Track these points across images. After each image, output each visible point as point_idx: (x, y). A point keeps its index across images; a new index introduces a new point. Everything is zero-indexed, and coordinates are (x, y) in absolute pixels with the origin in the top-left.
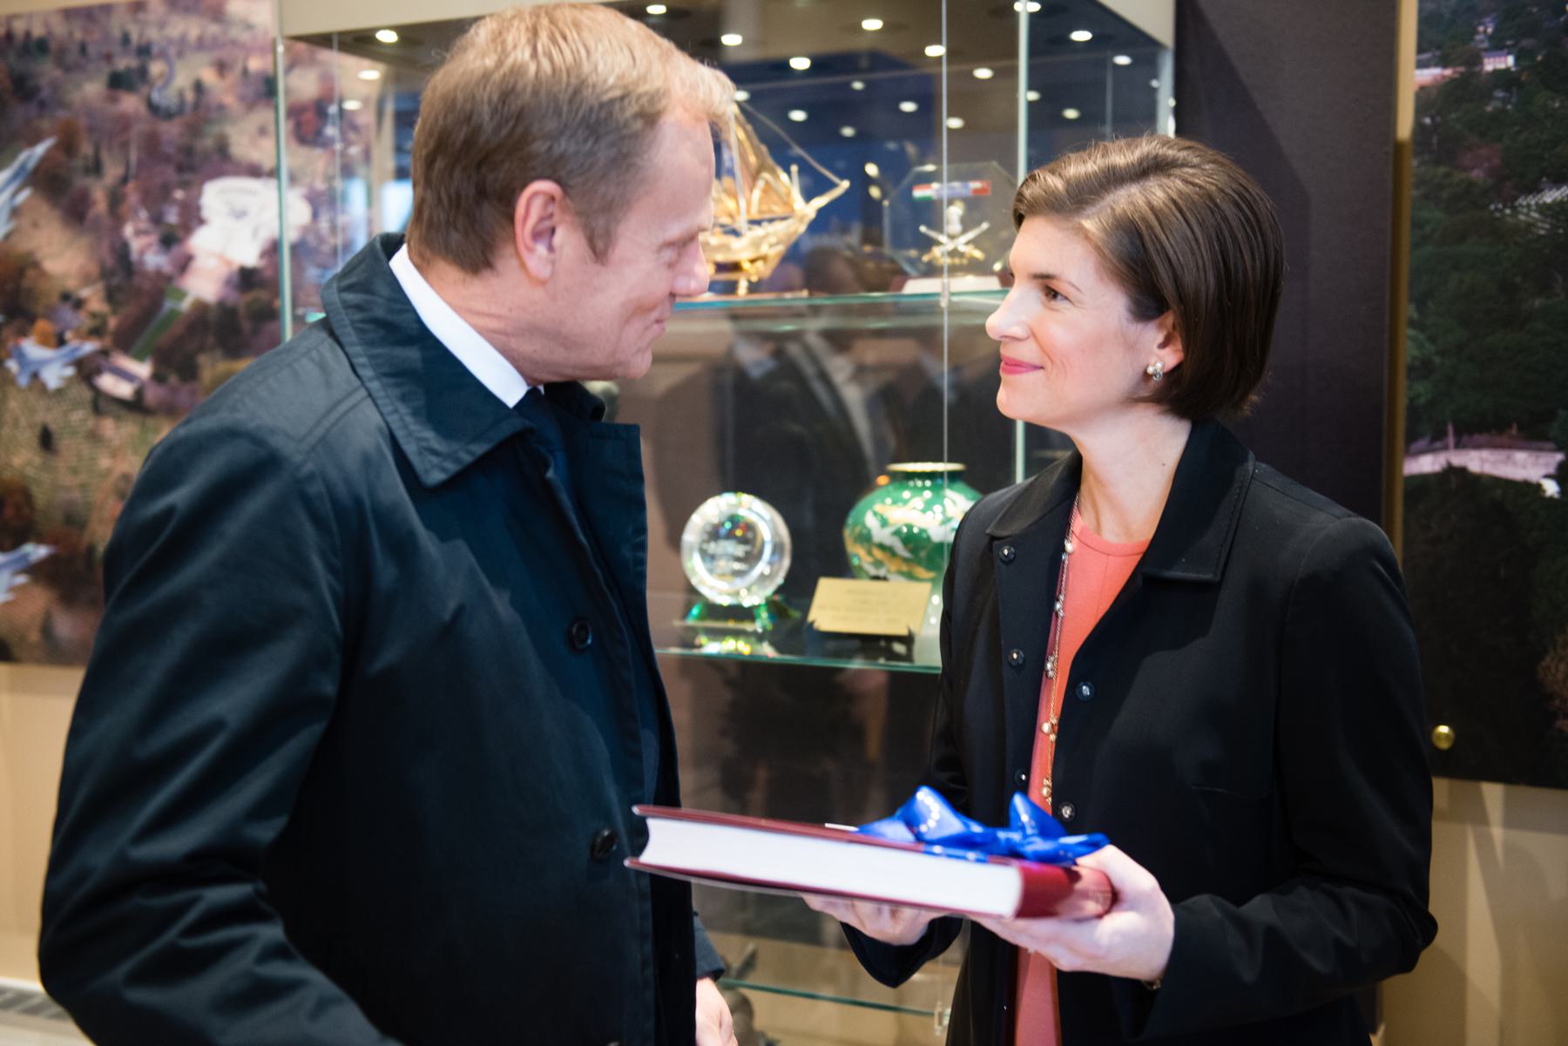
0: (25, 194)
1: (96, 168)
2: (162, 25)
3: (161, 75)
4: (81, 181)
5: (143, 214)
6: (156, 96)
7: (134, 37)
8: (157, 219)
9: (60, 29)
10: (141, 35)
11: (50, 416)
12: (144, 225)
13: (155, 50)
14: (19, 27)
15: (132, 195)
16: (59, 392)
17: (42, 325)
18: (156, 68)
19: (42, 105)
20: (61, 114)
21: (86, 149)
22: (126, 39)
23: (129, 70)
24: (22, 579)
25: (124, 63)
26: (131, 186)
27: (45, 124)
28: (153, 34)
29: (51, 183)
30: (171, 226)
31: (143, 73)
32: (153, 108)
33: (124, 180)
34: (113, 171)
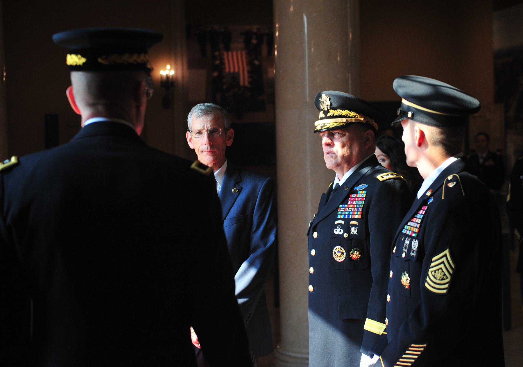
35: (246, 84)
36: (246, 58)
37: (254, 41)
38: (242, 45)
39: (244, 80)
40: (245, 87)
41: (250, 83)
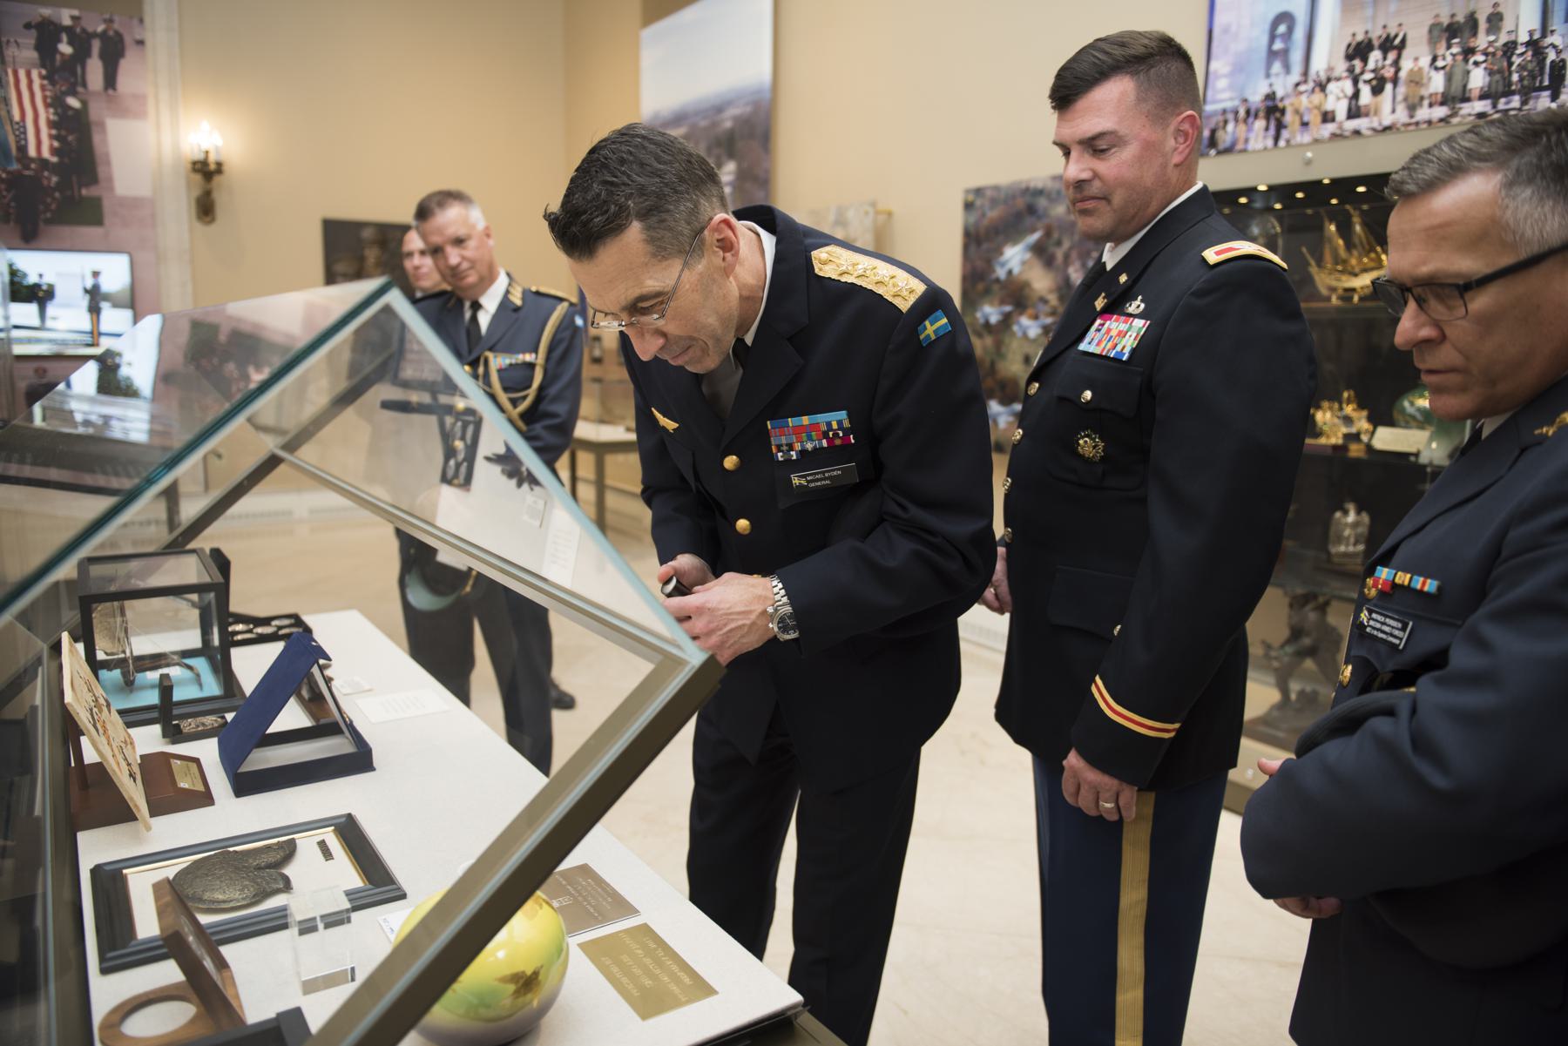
0: (1028, 256)
1: (1059, 243)
4: (1052, 249)
9: (1050, 185)
11: (1028, 349)
14: (1032, 185)
15: (1074, 255)
16: (1034, 341)
17: (1030, 311)
19: (1039, 218)
20: (1046, 221)
21: (1056, 235)
24: (1011, 419)
27: (1040, 225)
29: (1039, 250)
33: (1070, 249)
34: (1066, 244)
35: (46, 154)
36: (43, 88)
37: (65, 48)
38: (34, 55)
39: (41, 142)
40: (44, 163)
41: (54, 151)
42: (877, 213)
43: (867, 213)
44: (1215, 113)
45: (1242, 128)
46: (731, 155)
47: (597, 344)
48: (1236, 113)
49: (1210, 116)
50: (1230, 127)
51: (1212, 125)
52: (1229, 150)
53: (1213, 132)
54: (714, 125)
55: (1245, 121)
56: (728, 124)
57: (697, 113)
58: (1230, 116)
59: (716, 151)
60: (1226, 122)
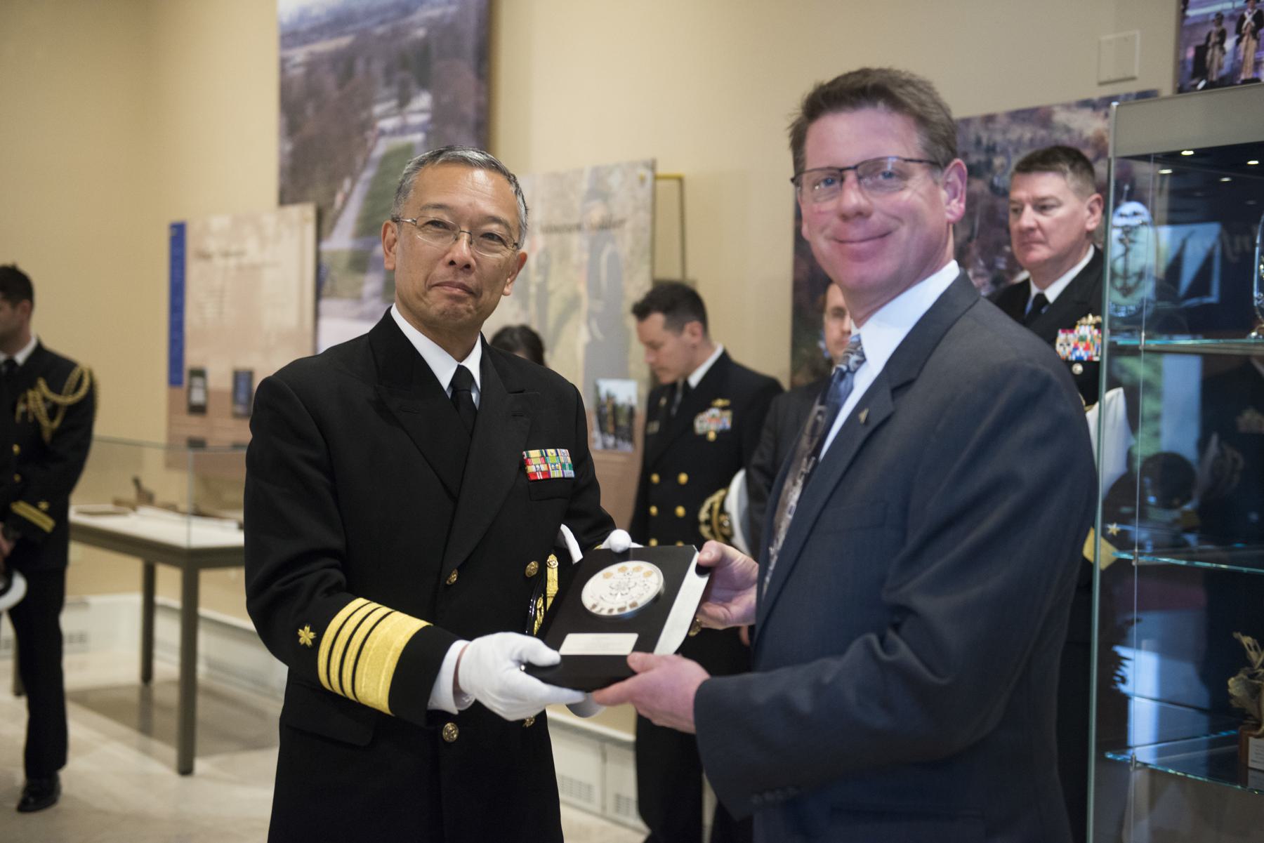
2: (1004, 132)
3: (1002, 166)
5: (981, 263)
6: (996, 181)
7: (985, 141)
8: (990, 267)
10: (989, 139)
12: (980, 270)
13: (998, 149)
15: (974, 250)
18: (998, 161)
22: (979, 142)
23: (979, 162)
25: (974, 159)
26: (974, 241)
28: (998, 138)
30: (1000, 270)
31: (989, 164)
32: (993, 187)
33: (969, 239)
42: (656, 178)
43: (642, 180)
44: (1204, 21)
45: (1249, 44)
46: (424, 84)
47: (198, 381)
48: (1243, 19)
49: (1195, 26)
50: (1229, 44)
51: (1202, 42)
52: (1227, 81)
53: (1201, 52)
54: (397, 33)
55: (1254, 33)
56: (421, 33)
57: (369, 14)
58: (1230, 26)
59: (400, 75)
60: (1222, 36)
